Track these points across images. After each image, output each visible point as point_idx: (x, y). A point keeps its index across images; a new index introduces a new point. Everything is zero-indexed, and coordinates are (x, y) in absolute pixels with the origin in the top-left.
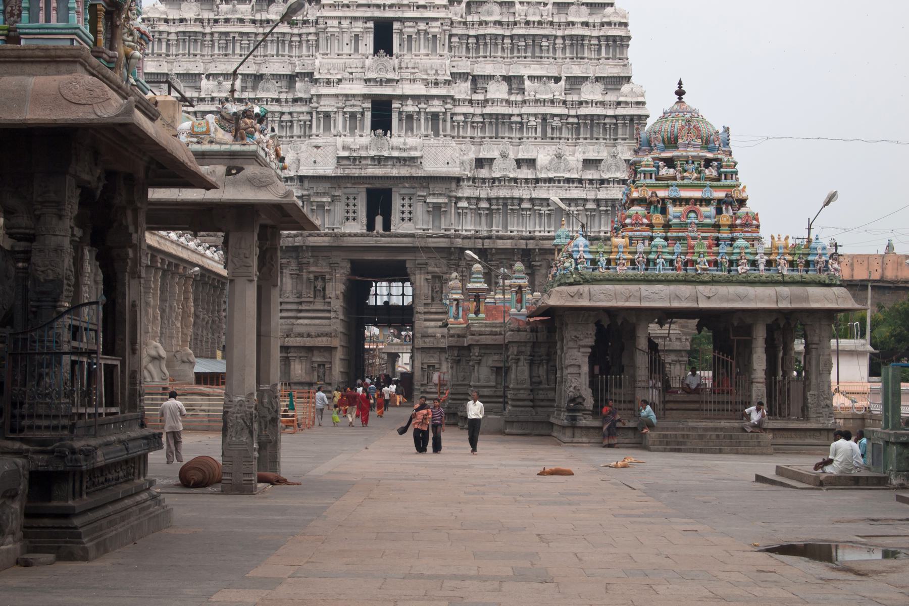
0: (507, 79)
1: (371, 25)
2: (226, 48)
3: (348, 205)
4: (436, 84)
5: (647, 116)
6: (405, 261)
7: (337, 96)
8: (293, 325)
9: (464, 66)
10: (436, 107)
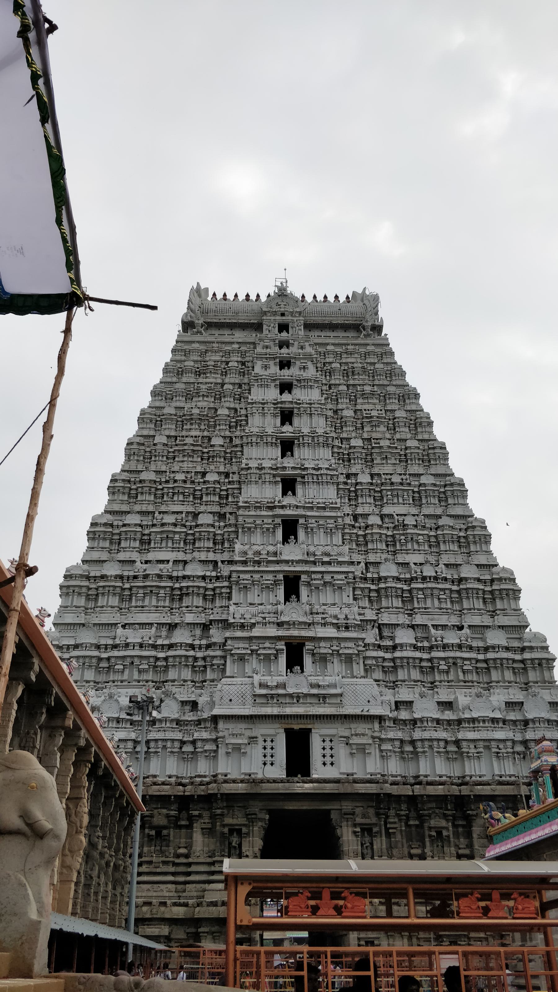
0: (413, 627)
2: (143, 600)
3: (265, 748)
4: (347, 628)
5: (554, 660)
6: (328, 812)
7: (250, 639)
8: (204, 890)
9: (370, 615)
10: (349, 649)
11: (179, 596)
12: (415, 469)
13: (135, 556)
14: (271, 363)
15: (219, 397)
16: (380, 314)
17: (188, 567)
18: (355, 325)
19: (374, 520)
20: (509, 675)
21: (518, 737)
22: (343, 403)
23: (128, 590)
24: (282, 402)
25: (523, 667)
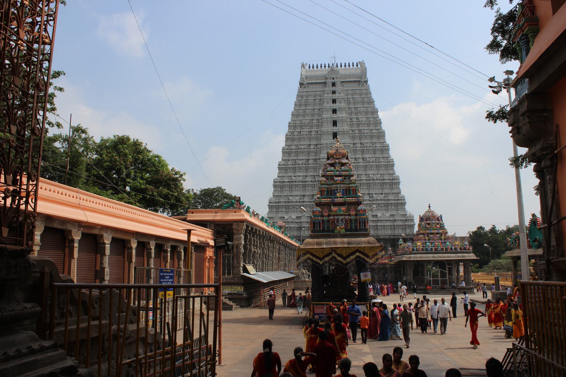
0: (369, 194)
11: (304, 186)
12: (375, 141)
13: (293, 175)
15: (313, 115)
16: (368, 76)
17: (307, 178)
19: (361, 160)
20: (393, 207)
21: (392, 224)
22: (354, 116)
23: (292, 186)
25: (397, 205)
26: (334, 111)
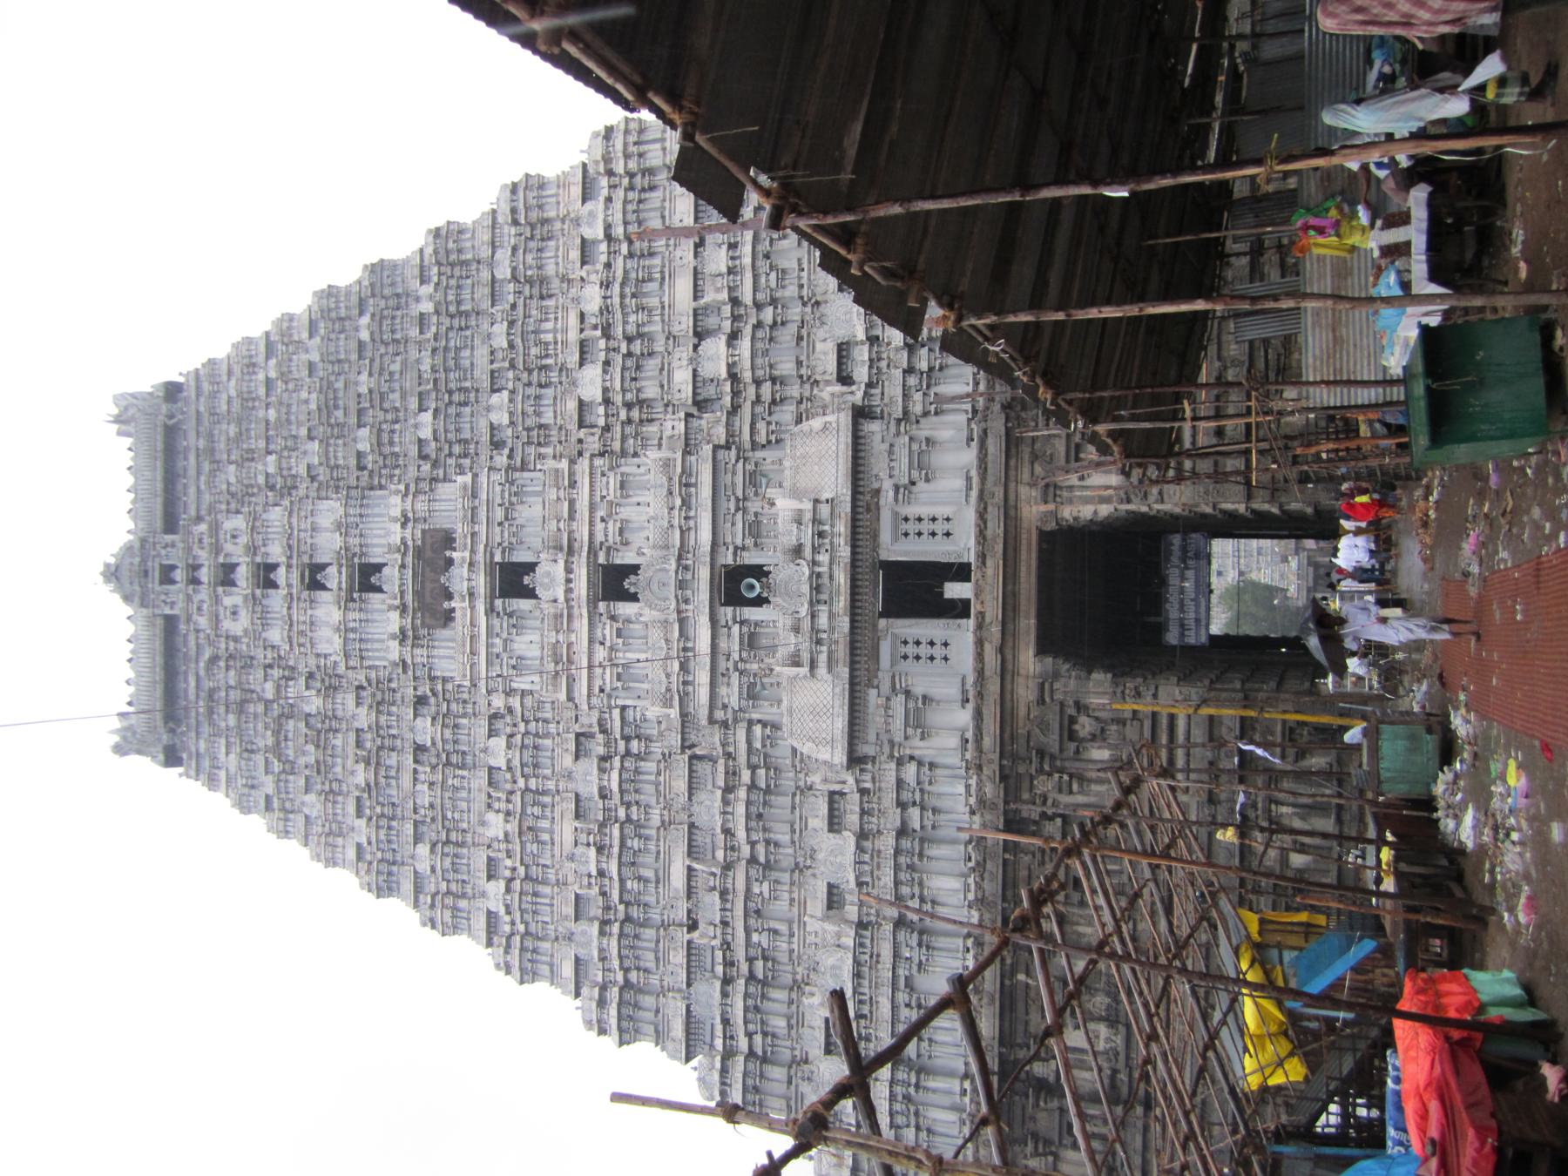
1: (602, 606)
14: (228, 601)
18: (174, 433)
24: (289, 586)
26: (265, 576)
